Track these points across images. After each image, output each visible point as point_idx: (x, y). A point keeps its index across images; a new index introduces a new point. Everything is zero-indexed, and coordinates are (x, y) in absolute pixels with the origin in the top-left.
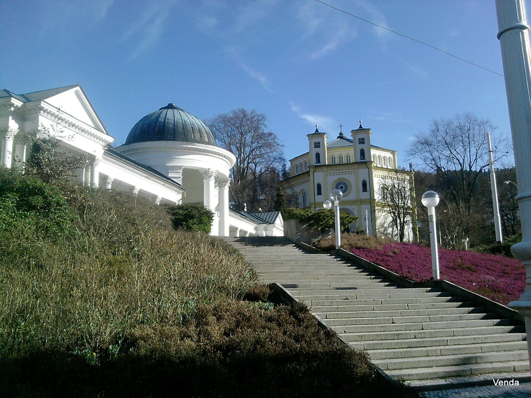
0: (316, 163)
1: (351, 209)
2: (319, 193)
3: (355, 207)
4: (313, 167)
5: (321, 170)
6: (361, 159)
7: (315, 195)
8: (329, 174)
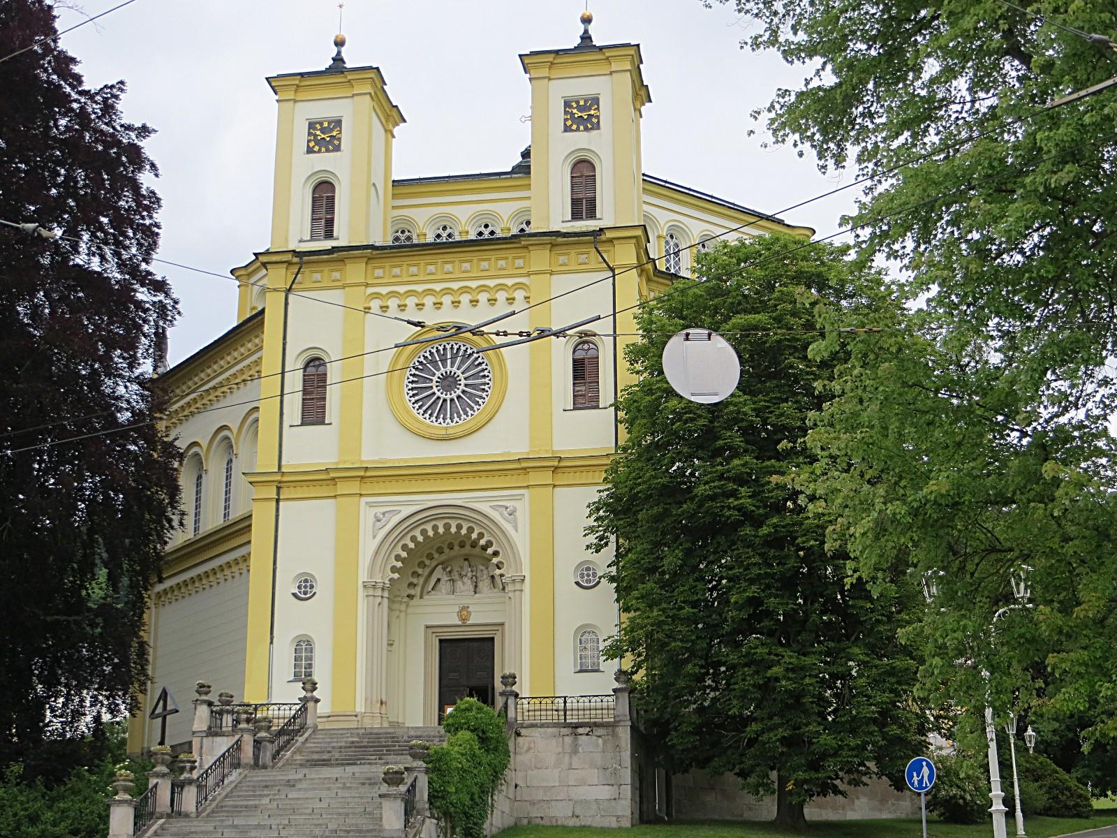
0: (312, 240)
1: (494, 515)
2: (314, 412)
3: (523, 504)
4: (288, 257)
5: (336, 275)
6: (576, 215)
7: (286, 425)
8: (375, 305)
